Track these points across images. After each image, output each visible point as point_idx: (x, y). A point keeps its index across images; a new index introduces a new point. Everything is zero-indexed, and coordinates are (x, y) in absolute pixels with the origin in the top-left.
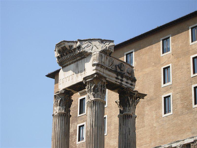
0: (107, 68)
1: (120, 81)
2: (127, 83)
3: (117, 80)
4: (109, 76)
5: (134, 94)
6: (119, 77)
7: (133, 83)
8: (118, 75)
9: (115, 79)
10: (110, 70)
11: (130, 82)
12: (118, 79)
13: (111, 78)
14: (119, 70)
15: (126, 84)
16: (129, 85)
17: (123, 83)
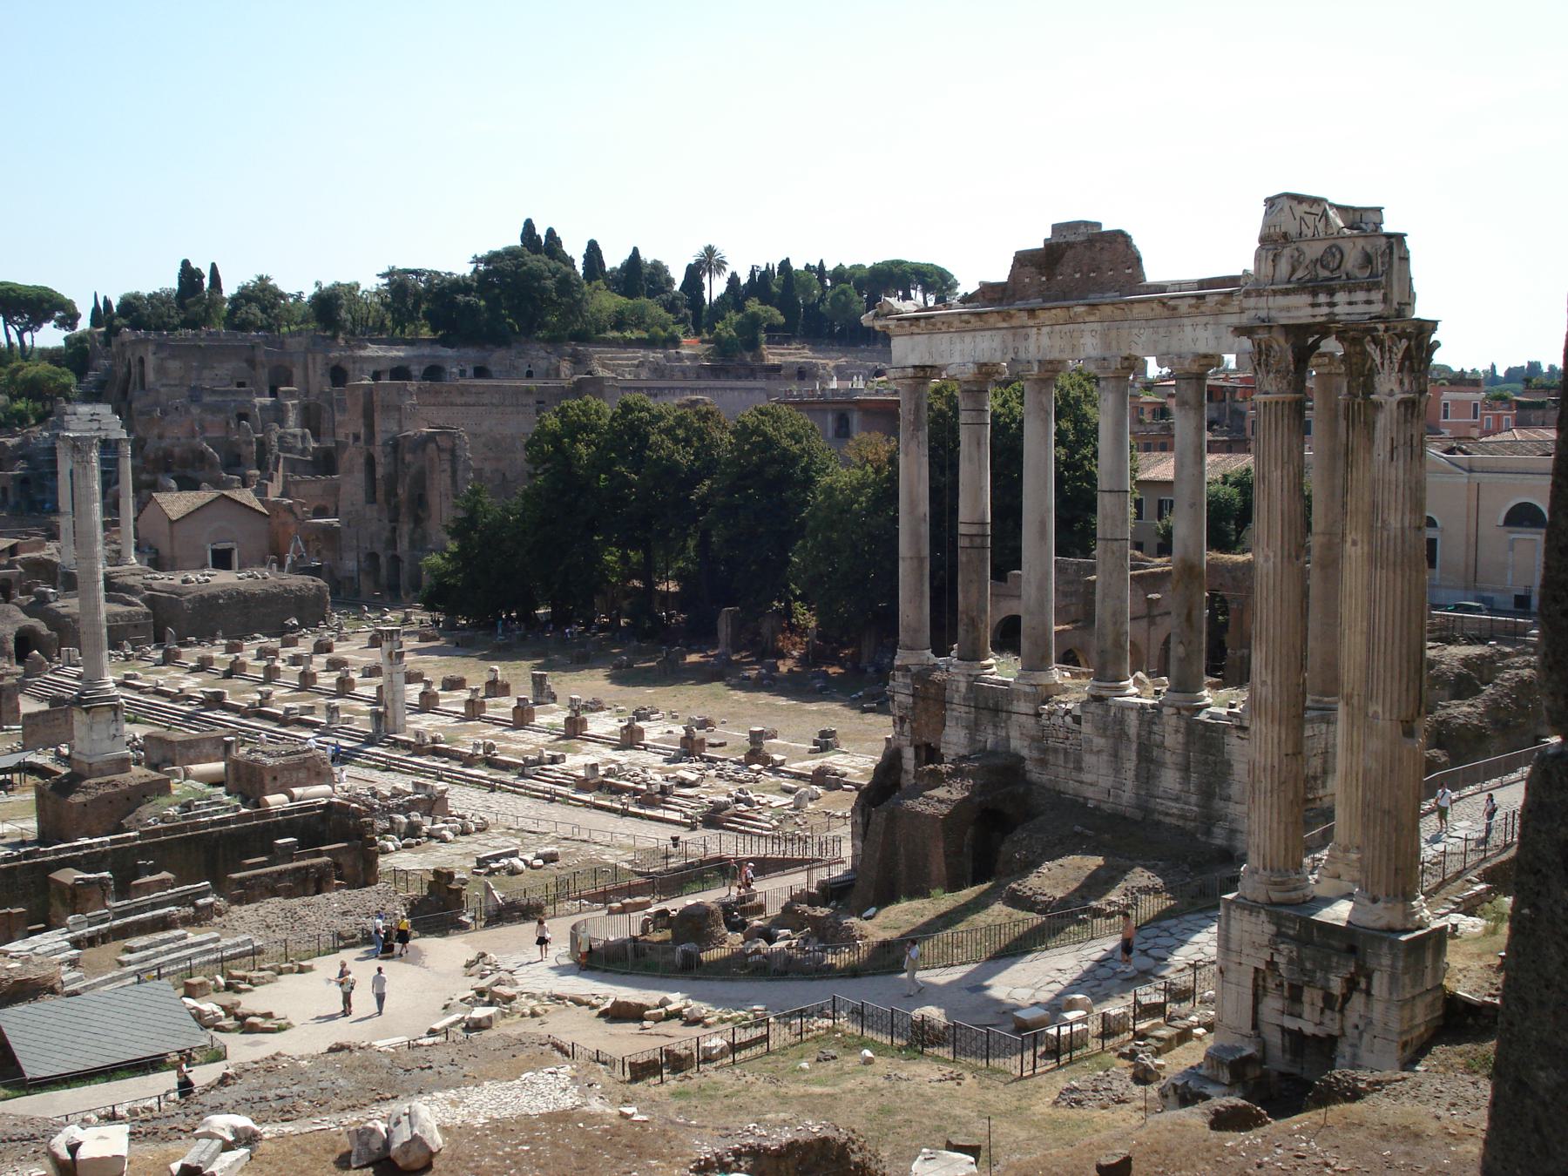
0: (1275, 293)
1: (1325, 310)
2: (1350, 303)
3: (1318, 311)
4: (1288, 309)
5: (1376, 329)
6: (1322, 298)
7: (1377, 296)
8: (1315, 294)
9: (1310, 311)
10: (1286, 292)
11: (1360, 296)
12: (1319, 305)
13: (1294, 313)
14: (1324, 273)
15: (1348, 309)
16: (1361, 308)
17: (1337, 310)
